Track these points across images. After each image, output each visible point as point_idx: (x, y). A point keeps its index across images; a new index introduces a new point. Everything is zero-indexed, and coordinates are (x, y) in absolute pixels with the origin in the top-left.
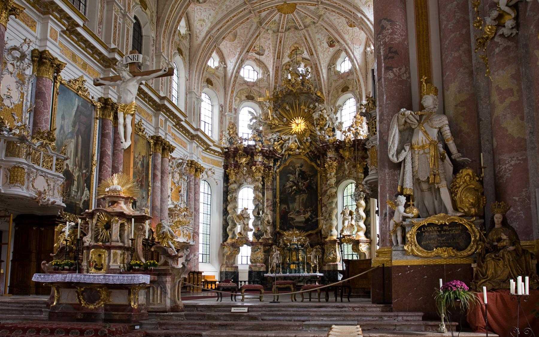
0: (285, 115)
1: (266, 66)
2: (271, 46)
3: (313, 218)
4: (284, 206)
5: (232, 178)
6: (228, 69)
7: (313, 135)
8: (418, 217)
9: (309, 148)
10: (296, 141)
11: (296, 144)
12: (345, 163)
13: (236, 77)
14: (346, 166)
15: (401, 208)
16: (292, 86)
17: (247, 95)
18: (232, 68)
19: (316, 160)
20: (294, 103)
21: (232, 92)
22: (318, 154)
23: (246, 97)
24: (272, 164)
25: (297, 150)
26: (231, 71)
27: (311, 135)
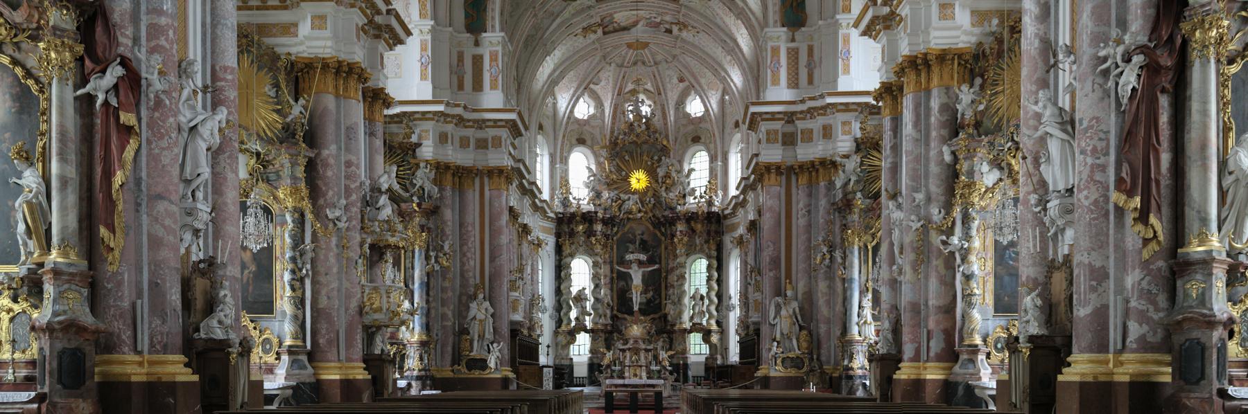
1: (599, 97)
2: (611, 79)
3: (655, 299)
4: (622, 283)
5: (567, 250)
6: (559, 105)
7: (656, 195)
9: (651, 211)
12: (697, 237)
13: (569, 118)
14: (698, 242)
17: (577, 137)
18: (564, 106)
21: (564, 136)
23: (577, 140)
24: (609, 232)
26: (563, 110)
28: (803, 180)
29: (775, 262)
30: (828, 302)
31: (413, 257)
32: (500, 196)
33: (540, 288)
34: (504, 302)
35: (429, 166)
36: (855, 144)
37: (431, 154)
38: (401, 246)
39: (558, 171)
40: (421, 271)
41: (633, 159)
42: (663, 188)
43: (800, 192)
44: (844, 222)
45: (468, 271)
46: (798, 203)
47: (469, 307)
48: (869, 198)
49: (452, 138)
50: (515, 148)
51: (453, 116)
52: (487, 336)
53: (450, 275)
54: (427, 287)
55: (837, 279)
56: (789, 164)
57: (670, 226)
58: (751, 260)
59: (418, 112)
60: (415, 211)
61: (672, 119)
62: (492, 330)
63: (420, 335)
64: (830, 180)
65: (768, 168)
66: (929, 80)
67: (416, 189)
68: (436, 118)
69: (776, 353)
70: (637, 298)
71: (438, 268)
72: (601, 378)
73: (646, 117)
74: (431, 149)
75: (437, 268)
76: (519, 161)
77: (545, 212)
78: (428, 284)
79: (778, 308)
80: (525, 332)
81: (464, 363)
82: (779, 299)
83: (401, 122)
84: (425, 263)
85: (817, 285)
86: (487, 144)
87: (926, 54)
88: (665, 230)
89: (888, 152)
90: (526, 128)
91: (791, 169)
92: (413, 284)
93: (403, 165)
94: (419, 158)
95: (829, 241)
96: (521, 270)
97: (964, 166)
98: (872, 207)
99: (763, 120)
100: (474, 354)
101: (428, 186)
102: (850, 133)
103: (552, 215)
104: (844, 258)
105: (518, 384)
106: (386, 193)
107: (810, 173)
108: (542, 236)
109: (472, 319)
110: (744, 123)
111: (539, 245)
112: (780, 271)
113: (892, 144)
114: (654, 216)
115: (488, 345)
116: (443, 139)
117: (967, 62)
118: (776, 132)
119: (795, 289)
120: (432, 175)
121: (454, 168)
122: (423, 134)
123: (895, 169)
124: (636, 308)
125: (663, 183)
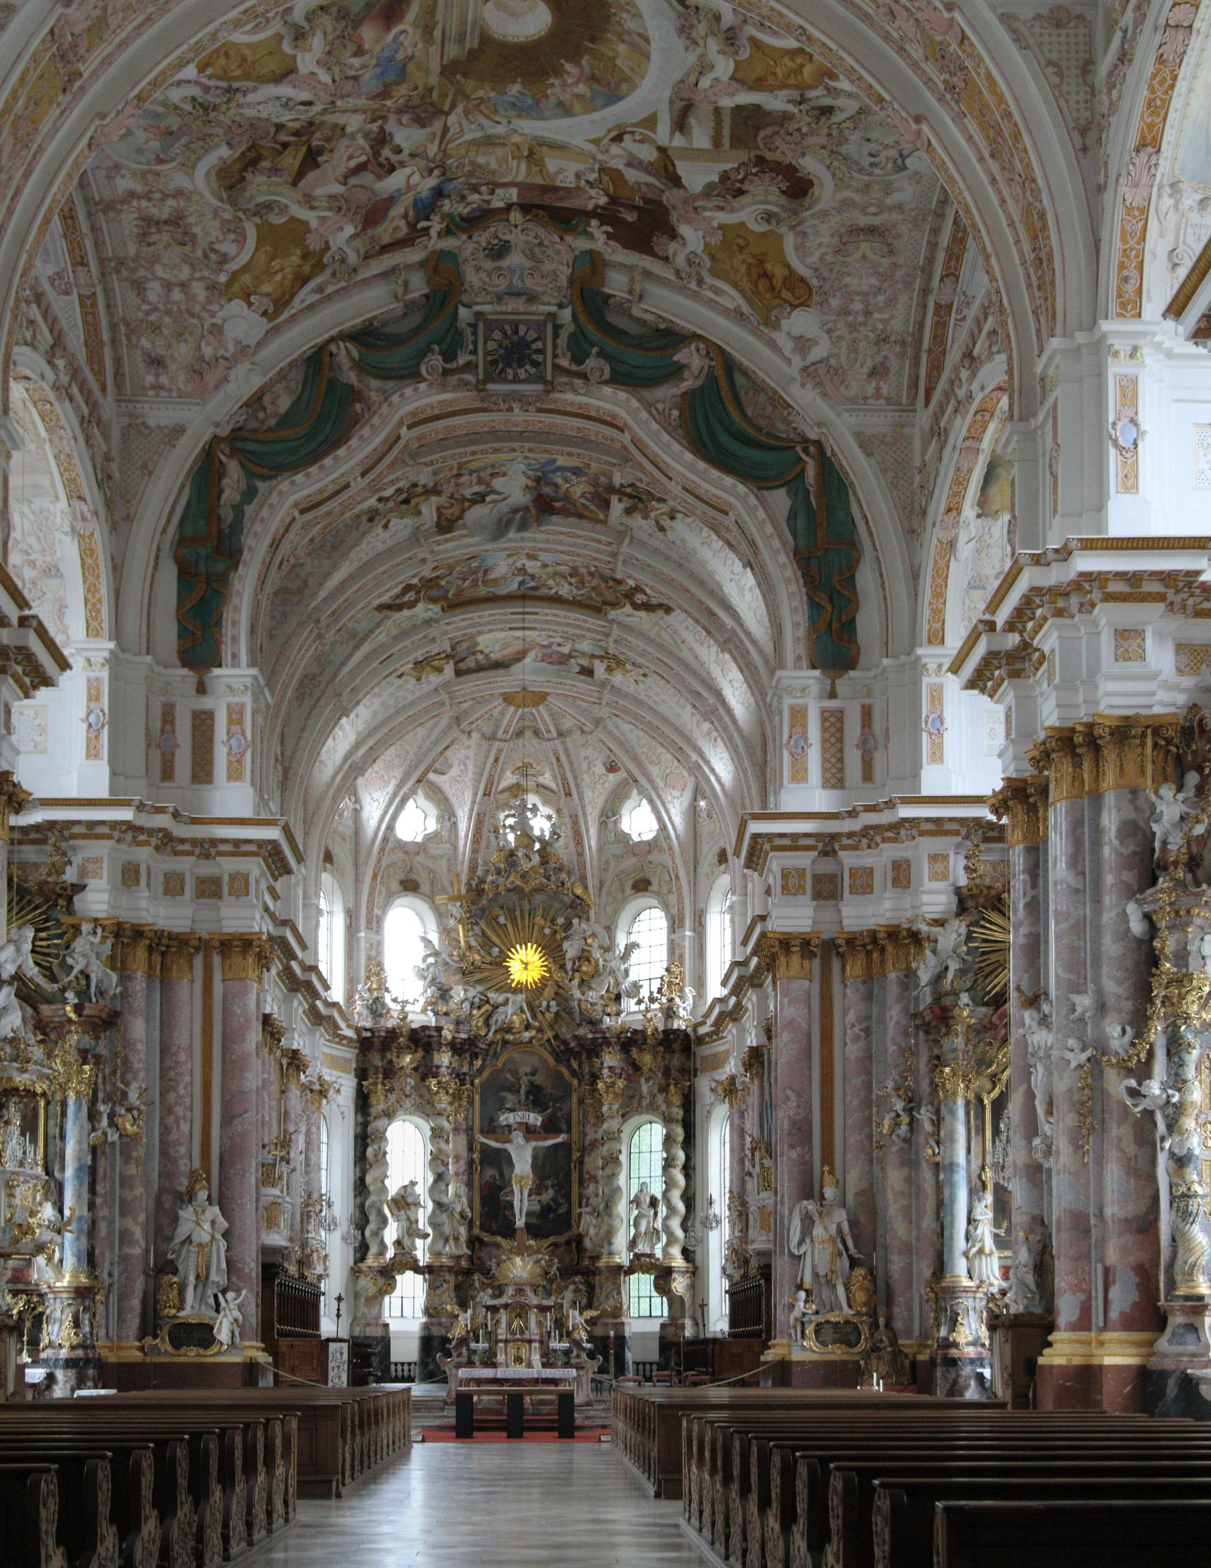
8: (817, 1313)
12: (643, 1080)
15: (802, 1304)
28: (855, 968)
29: (801, 1130)
30: (907, 1212)
31: (64, 1114)
32: (244, 993)
33: (323, 1179)
34: (250, 1206)
35: (99, 931)
36: (955, 900)
37: (105, 907)
38: (39, 1091)
39: (363, 945)
40: (80, 1142)
43: (848, 991)
44: (936, 1051)
45: (177, 1143)
46: (845, 1013)
47: (176, 1219)
48: (986, 1004)
49: (149, 874)
50: (275, 896)
51: (151, 832)
52: (214, 1277)
53: (139, 1152)
54: (91, 1175)
55: (924, 1164)
56: (825, 936)
58: (751, 1125)
59: (79, 822)
60: (70, 1021)
62: (224, 1266)
63: (75, 1275)
64: (909, 968)
65: (785, 943)
66: (1098, 776)
67: (72, 977)
68: (116, 834)
69: (804, 1314)
70: (522, 1203)
71: (116, 1137)
72: (448, 1365)
74: (105, 897)
75: (113, 1136)
76: (285, 923)
77: (336, 1027)
78: (93, 1171)
79: (808, 1223)
80: (293, 1269)
81: (165, 1333)
82: (810, 1206)
83: (44, 841)
84: (87, 1126)
85: (885, 1178)
86: (220, 888)
87: (1091, 726)
89: (1021, 914)
90: (300, 859)
91: (830, 946)
92: (63, 1169)
93: (47, 929)
94: (78, 915)
95: (908, 1089)
96: (285, 1143)
97: (1168, 943)
98: (991, 1022)
99: (776, 848)
100: (191, 1311)
101: (98, 971)
102: (945, 877)
103: (350, 1033)
104: (937, 1122)
105: (276, 1375)
106: (10, 984)
107: (869, 953)
108: (328, 1075)
109: (183, 1243)
110: (737, 853)
111: (323, 1093)
112: (811, 1149)
113: (1028, 898)
115: (216, 1297)
116: (130, 876)
117: (1169, 741)
118: (801, 872)
119: (841, 1185)
120: (107, 949)
121: (151, 935)
122: (90, 867)
123: (1035, 948)
124: (520, 1222)
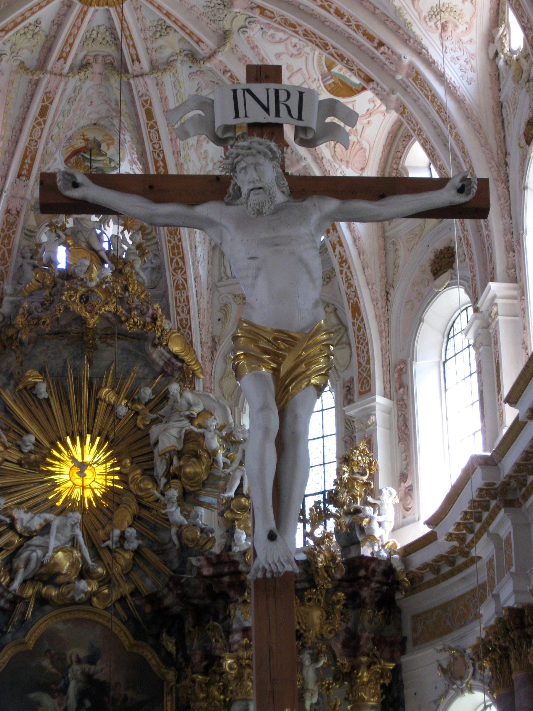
0: (27, 422)
10: (73, 540)
11: (76, 554)
12: (306, 658)
14: (310, 674)
16: (85, 299)
19: (158, 637)
20: (70, 373)
22: (177, 609)
25: (83, 584)
27: (137, 518)
41: (64, 399)
42: (174, 493)
57: (199, 623)
61: (203, 272)
73: (114, 259)
88: (181, 645)
114: (135, 593)
125: (171, 476)
